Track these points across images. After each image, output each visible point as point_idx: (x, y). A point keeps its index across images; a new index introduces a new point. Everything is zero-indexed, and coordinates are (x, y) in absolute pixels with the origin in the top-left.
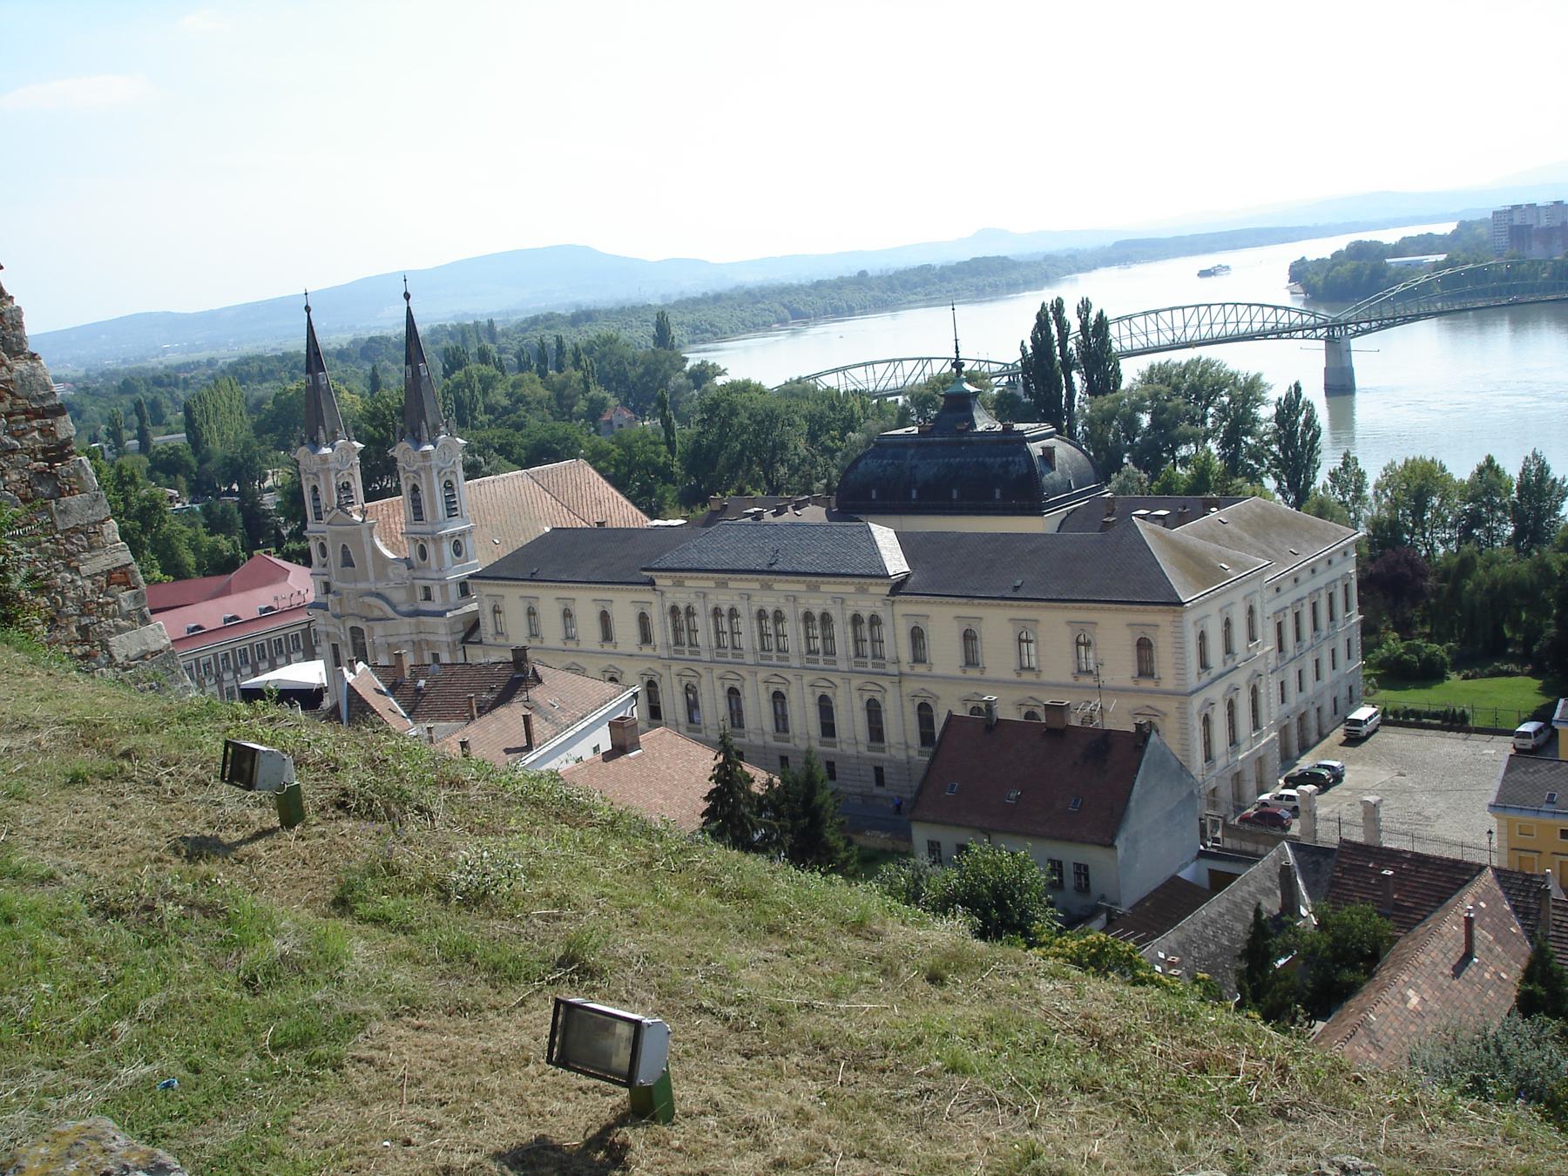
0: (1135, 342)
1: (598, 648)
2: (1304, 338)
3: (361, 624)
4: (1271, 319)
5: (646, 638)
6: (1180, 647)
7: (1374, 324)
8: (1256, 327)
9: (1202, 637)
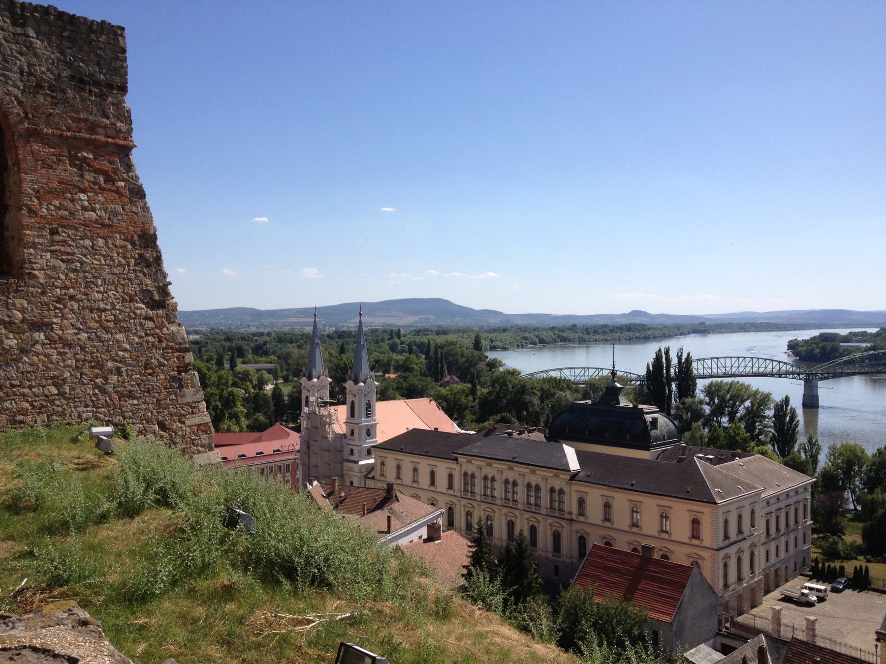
2: (793, 378)
5: (450, 487)
8: (769, 370)
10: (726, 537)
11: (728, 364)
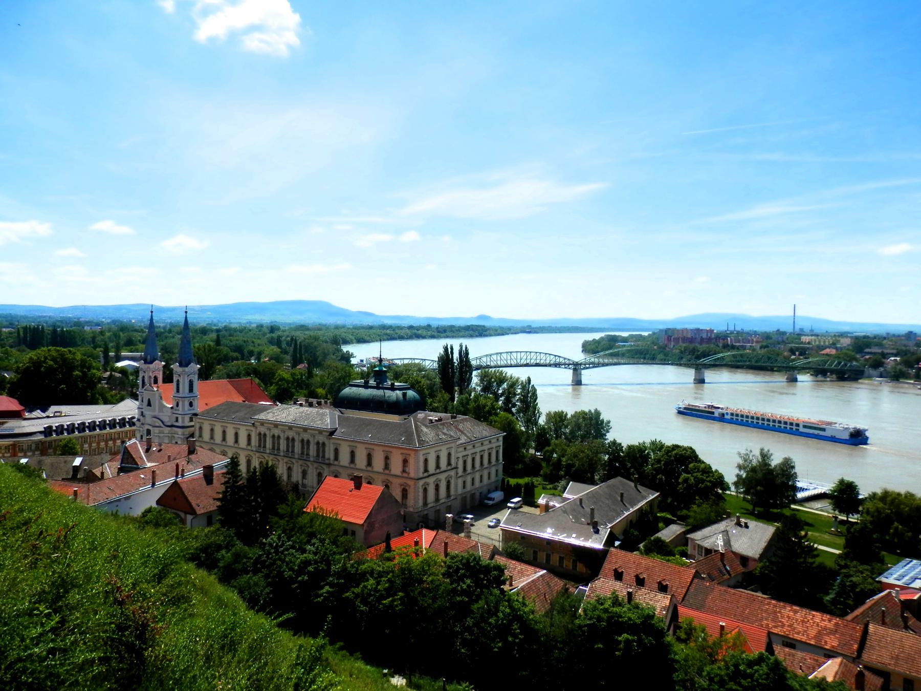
0: (492, 363)
1: (233, 445)
2: (565, 368)
4: (553, 360)
5: (249, 443)
6: (417, 462)
7: (591, 366)
8: (548, 362)
9: (426, 461)
10: (426, 470)
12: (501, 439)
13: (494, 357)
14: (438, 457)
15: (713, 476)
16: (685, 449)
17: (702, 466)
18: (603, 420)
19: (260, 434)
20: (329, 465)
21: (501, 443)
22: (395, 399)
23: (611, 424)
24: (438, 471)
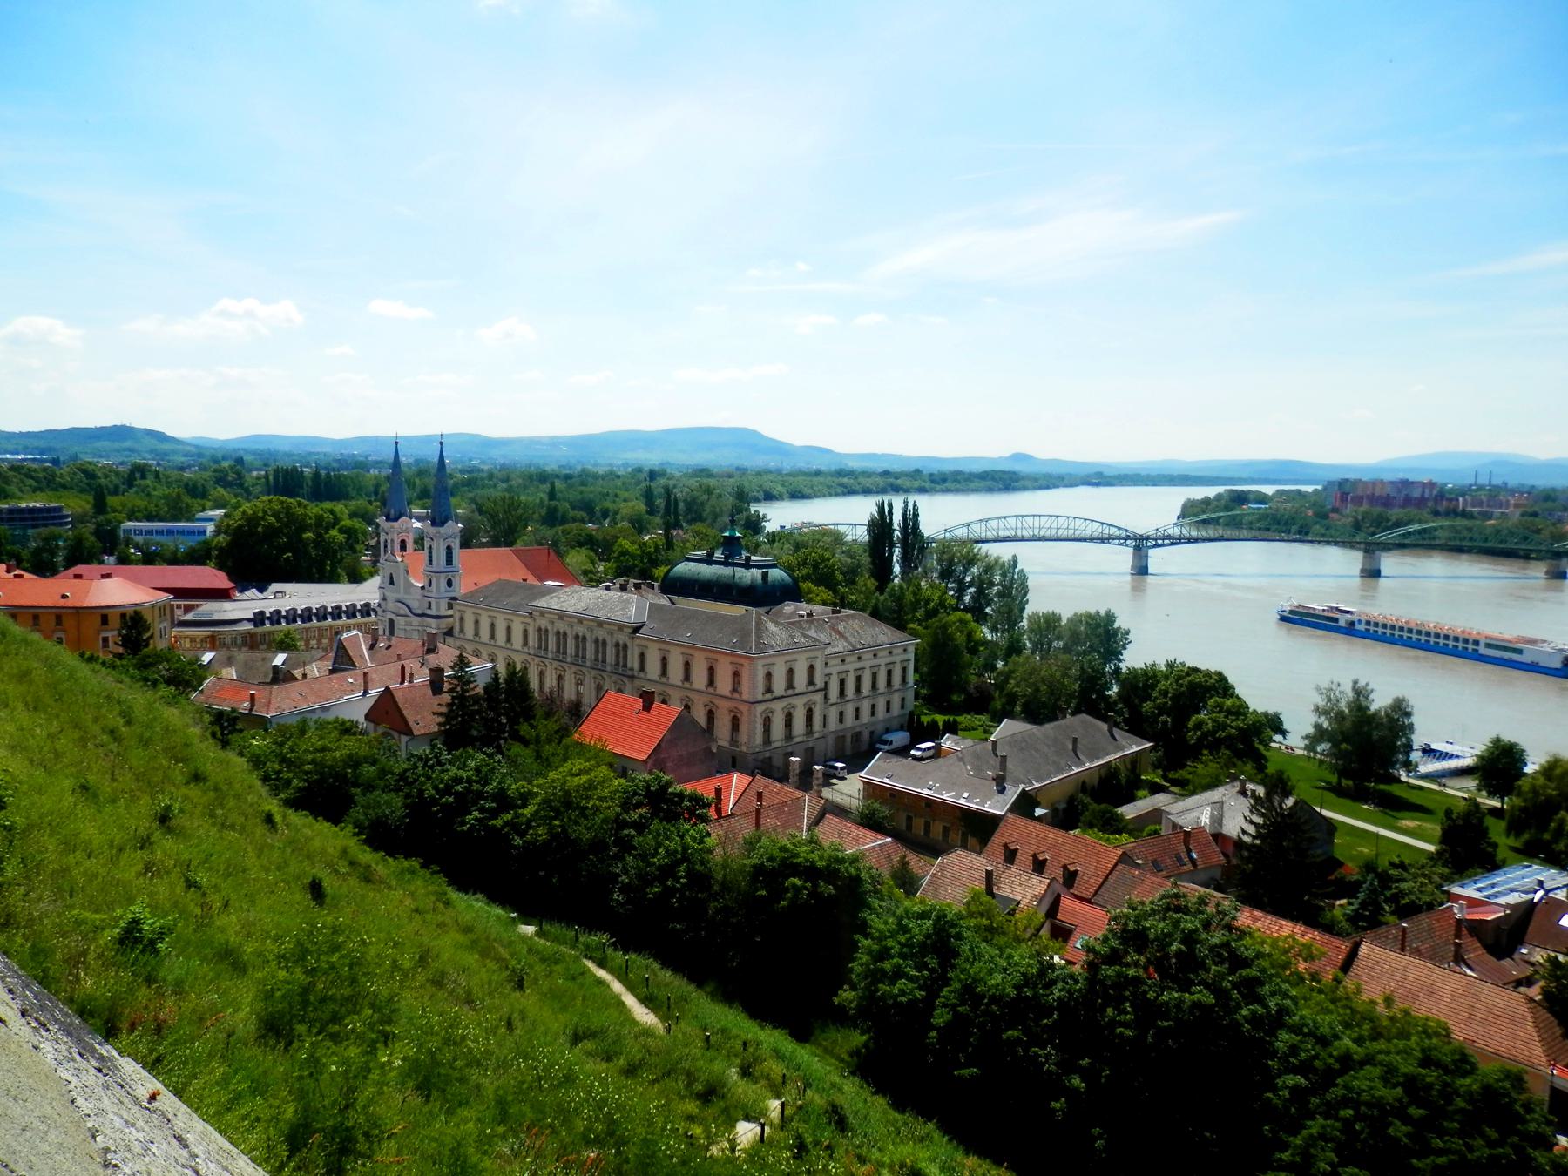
3: (393, 617)
5: (525, 643)
6: (753, 675)
9: (769, 676)
10: (769, 690)
11: (1037, 525)
12: (912, 649)
13: (994, 524)
14: (791, 672)
15: (1244, 720)
16: (1208, 674)
17: (1229, 702)
18: (1119, 628)
19: (540, 630)
20: (632, 677)
21: (912, 656)
22: (749, 582)
23: (1130, 636)
24: (790, 692)
